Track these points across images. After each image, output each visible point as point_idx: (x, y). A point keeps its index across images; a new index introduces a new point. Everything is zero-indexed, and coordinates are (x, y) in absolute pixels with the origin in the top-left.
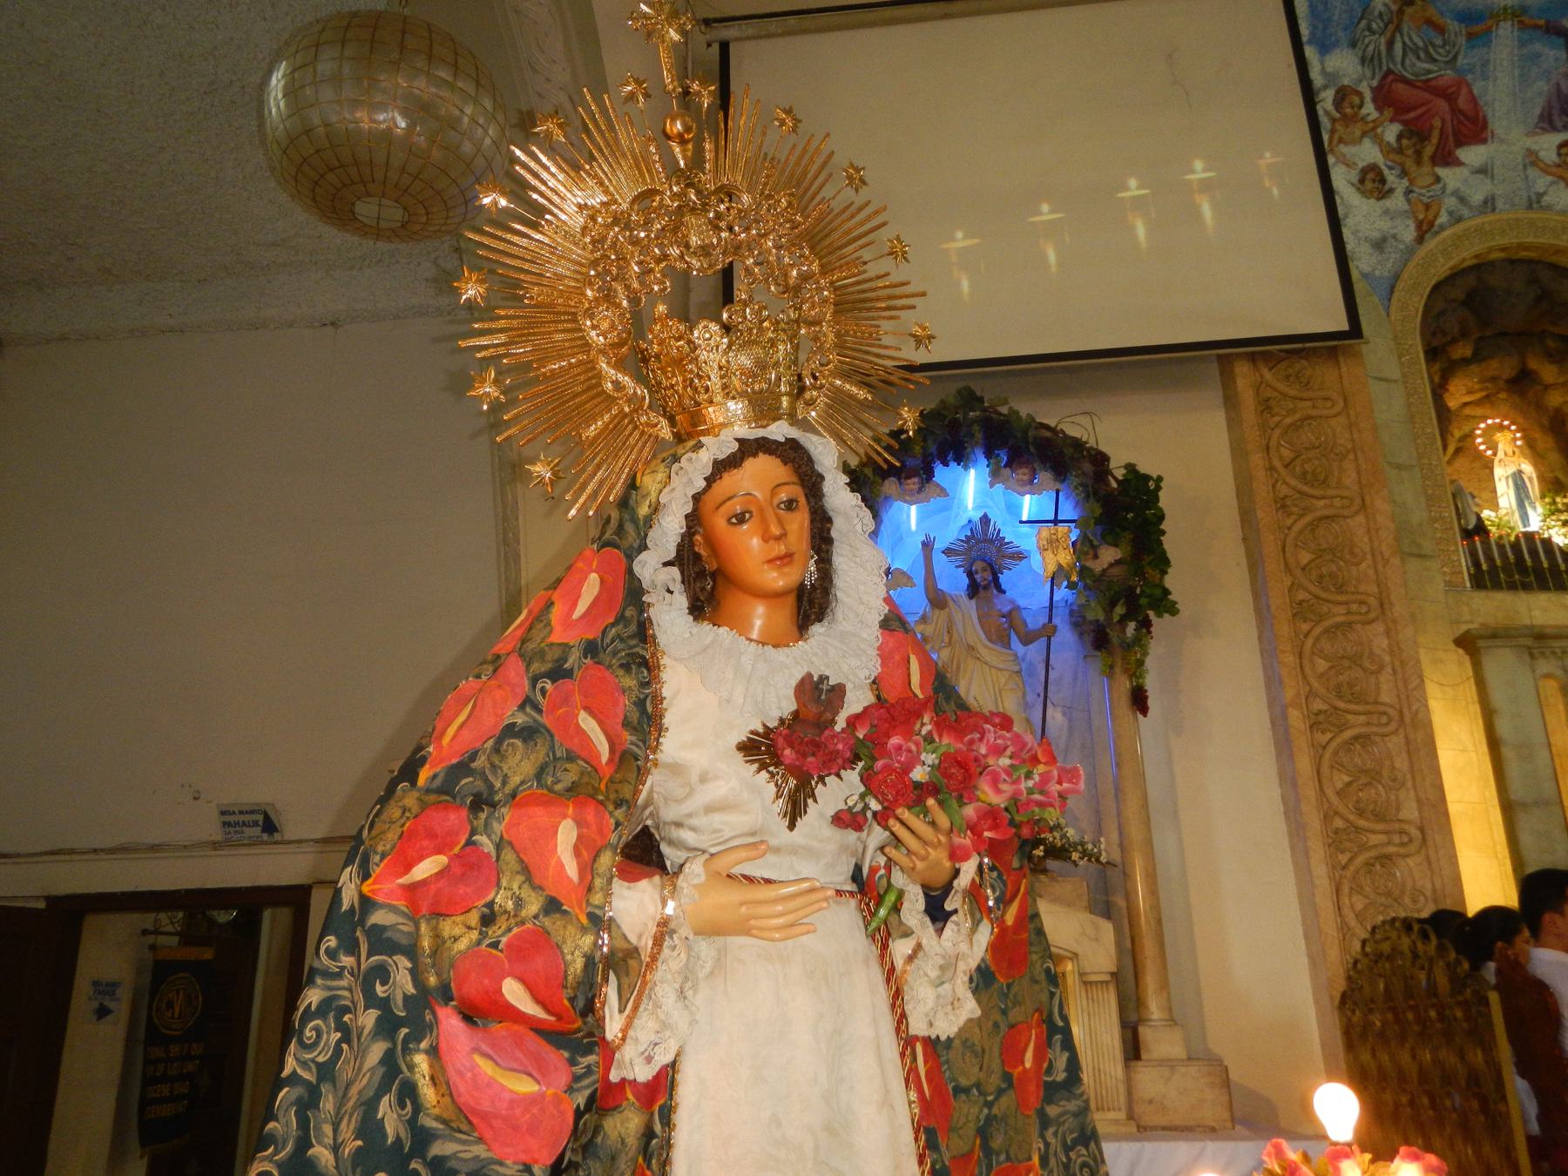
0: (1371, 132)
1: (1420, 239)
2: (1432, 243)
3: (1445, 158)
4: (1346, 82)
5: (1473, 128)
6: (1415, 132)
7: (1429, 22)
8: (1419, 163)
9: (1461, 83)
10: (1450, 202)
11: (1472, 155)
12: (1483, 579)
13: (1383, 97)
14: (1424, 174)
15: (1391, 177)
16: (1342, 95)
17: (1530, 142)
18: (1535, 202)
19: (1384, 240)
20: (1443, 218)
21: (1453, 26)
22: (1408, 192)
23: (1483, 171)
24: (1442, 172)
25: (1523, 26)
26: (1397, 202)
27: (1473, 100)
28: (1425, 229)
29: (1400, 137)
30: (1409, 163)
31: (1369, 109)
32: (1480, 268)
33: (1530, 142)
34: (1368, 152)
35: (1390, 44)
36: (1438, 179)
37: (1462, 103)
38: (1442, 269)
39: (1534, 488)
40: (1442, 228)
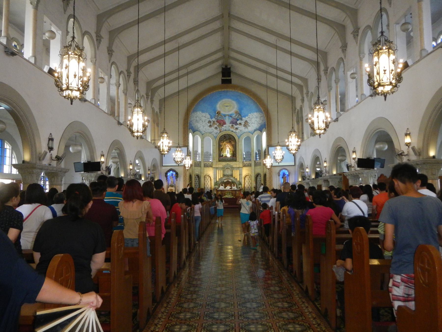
0: (216, 124)
1: (220, 133)
2: (220, 133)
3: (222, 126)
5: (225, 123)
6: (220, 124)
10: (223, 129)
11: (225, 126)
12: (219, 161)
13: (217, 121)
14: (220, 127)
15: (218, 128)
16: (213, 122)
17: (229, 125)
20: (222, 131)
21: (223, 116)
24: (222, 127)
26: (218, 129)
28: (220, 132)
31: (216, 122)
33: (229, 125)
34: (216, 126)
37: (224, 121)
39: (229, 152)
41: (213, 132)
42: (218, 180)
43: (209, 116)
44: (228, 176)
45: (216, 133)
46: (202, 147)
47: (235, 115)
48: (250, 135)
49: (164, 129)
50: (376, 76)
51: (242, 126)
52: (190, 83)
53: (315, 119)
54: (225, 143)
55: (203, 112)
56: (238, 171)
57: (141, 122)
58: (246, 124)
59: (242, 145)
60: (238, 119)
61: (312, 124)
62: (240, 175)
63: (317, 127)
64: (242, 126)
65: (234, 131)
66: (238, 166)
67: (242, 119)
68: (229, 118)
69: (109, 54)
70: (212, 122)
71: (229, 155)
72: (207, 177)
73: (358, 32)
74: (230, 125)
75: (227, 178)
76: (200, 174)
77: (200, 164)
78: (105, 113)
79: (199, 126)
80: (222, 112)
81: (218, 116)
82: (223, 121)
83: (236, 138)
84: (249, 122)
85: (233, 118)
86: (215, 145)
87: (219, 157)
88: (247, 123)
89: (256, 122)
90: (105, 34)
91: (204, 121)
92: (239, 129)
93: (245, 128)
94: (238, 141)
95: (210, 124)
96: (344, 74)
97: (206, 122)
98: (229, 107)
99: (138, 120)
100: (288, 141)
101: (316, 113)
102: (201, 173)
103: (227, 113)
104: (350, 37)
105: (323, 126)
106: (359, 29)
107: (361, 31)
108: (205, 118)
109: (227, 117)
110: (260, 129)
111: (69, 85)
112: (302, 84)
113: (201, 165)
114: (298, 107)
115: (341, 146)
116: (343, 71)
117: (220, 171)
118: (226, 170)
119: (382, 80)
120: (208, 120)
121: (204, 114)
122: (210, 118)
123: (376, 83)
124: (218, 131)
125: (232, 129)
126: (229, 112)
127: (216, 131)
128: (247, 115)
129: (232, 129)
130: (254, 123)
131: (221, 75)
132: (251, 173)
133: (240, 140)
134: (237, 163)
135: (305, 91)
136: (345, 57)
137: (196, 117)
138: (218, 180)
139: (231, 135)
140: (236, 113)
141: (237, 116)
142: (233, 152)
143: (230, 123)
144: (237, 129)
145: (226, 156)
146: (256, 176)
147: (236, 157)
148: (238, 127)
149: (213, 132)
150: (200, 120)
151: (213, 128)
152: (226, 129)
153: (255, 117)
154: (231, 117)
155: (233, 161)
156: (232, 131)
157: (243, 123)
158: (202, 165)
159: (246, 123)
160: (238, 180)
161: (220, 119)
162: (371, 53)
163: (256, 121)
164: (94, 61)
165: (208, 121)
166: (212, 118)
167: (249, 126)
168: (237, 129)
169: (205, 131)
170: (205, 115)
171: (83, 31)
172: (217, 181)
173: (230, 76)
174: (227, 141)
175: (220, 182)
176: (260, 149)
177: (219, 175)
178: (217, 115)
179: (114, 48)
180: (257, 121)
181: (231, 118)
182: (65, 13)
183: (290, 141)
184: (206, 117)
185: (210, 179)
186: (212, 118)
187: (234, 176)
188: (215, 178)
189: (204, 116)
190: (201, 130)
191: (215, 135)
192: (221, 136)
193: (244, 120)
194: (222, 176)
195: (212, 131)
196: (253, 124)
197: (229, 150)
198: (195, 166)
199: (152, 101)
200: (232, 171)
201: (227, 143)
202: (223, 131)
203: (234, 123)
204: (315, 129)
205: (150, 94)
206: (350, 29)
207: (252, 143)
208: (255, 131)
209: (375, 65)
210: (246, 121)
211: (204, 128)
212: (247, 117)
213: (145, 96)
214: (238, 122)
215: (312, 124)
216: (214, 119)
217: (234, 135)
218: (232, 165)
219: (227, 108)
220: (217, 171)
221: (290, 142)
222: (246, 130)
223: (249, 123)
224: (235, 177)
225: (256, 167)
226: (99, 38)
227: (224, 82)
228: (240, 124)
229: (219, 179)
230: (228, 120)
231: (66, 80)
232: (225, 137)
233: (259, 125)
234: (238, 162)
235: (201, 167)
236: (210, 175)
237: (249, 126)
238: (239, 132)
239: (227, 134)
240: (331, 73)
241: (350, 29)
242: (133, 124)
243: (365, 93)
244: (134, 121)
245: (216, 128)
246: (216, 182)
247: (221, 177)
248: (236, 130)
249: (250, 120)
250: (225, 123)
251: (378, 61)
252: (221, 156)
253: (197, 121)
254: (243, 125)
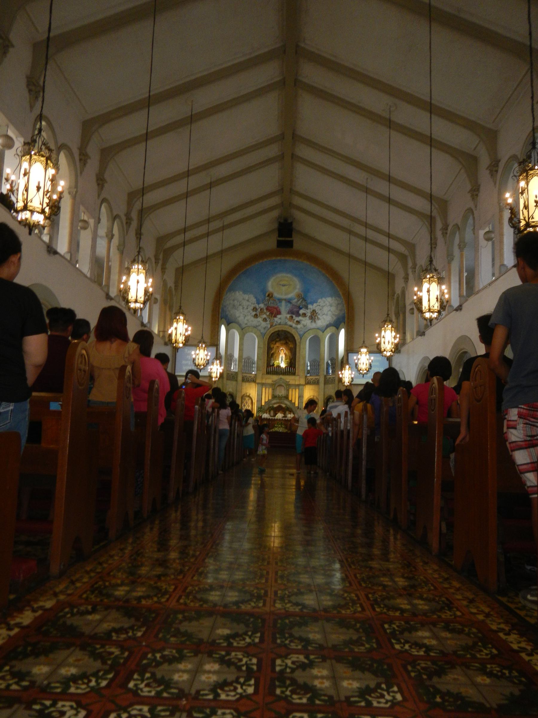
0: (265, 313)
1: (271, 327)
3: (275, 316)
4: (262, 307)
5: (279, 313)
6: (272, 313)
7: (274, 300)
8: (272, 317)
9: (278, 307)
10: (275, 323)
11: (279, 316)
12: (268, 373)
13: (267, 309)
14: (272, 318)
15: (268, 319)
17: (286, 315)
18: (286, 324)
19: (265, 328)
20: (274, 324)
21: (277, 300)
22: (270, 321)
23: (280, 318)
25: (286, 301)
26: (268, 322)
27: (279, 309)
28: (271, 326)
29: (269, 314)
30: (270, 317)
31: (265, 311)
32: (279, 331)
33: (286, 315)
34: (265, 316)
35: (268, 302)
36: (274, 319)
38: (273, 332)
39: (284, 359)
40: (274, 326)
41: (259, 325)
42: (263, 404)
43: (254, 300)
44: (280, 398)
45: (265, 328)
46: (241, 350)
47: (296, 300)
48: (320, 333)
49: (179, 308)
50: (522, 211)
51: (307, 318)
52: (226, 245)
53: (424, 294)
54: (278, 344)
55: (245, 292)
56: (297, 390)
57: (142, 286)
58: (314, 316)
59: (305, 348)
60: (301, 306)
61: (418, 303)
62: (301, 397)
63: (427, 308)
64: (307, 318)
65: (294, 325)
66: (297, 383)
67: (307, 308)
68: (286, 306)
69: (98, 184)
70: (259, 310)
71: (283, 365)
72: (247, 399)
73: (498, 166)
74: (288, 316)
75: (278, 401)
76: (235, 393)
77: (235, 377)
78: (86, 276)
79: (237, 315)
80: (276, 295)
81: (269, 300)
82: (276, 308)
83: (297, 337)
84: (319, 312)
85: (293, 305)
86: (262, 346)
87: (267, 367)
88: (315, 314)
89: (330, 312)
90: (93, 152)
91: (246, 307)
92: (303, 322)
93: (312, 322)
94: (300, 343)
95: (254, 313)
96: (474, 234)
97: (249, 309)
98: (287, 287)
99: (138, 282)
100: (380, 336)
101: (426, 286)
102: (236, 391)
103: (284, 297)
104: (484, 175)
105: (436, 306)
106: (500, 161)
107: (502, 165)
108: (248, 303)
109: (283, 303)
110: (337, 325)
111: (27, 203)
112: (406, 253)
113: (237, 378)
114: (398, 291)
115: (466, 351)
116: (472, 230)
117: (267, 389)
118: (278, 388)
119: (533, 218)
120: (253, 306)
121: (246, 297)
122: (256, 302)
123: (523, 223)
124: (267, 324)
125: (290, 323)
126: (286, 294)
127: (264, 324)
128: (315, 302)
129: (290, 323)
130: (327, 315)
131: (276, 234)
132: (319, 395)
133: (302, 341)
134: (297, 378)
135: (410, 264)
136: (476, 206)
137: (234, 300)
138: (263, 404)
139: (289, 333)
140: (299, 296)
141: (300, 302)
142: (291, 360)
143: (288, 313)
144: (298, 322)
145: (279, 366)
146: (326, 401)
147: (295, 367)
148: (301, 320)
149: (259, 325)
150: (240, 305)
151: (260, 319)
152: (280, 323)
153: (328, 304)
154: (291, 303)
155: (289, 375)
156: (291, 326)
157: (309, 314)
158: (240, 378)
159: (313, 314)
160: (297, 405)
161: (272, 305)
162: (515, 176)
163: (330, 310)
164: (74, 193)
165: (253, 308)
166: (258, 303)
167: (318, 319)
168: (298, 322)
169: (246, 324)
170: (248, 297)
171: (59, 145)
172: (261, 405)
173: (291, 236)
174: (282, 342)
175: (267, 407)
176: (335, 357)
177: (266, 396)
178: (267, 298)
179: (107, 176)
180: (331, 312)
181: (289, 305)
182: (31, 111)
183: (382, 336)
184: (249, 300)
185: (250, 401)
186: (258, 303)
187: (290, 399)
188: (259, 400)
189: (247, 299)
190: (241, 322)
191: (262, 331)
192: (272, 334)
193: (311, 309)
194: (270, 398)
195: (258, 325)
196: (324, 316)
197: (284, 356)
198: (227, 379)
199: (163, 269)
200: (288, 391)
201: (282, 344)
202: (276, 325)
203: (295, 312)
204: (424, 311)
205: (161, 256)
206: (485, 161)
207: (322, 346)
208: (328, 326)
209: (522, 193)
210: (314, 311)
211: (246, 318)
212: (315, 305)
213: (153, 260)
214: (301, 312)
215: (418, 303)
216: (262, 305)
217: (293, 332)
218: (288, 380)
219: (284, 288)
220: (264, 389)
221: (383, 337)
222: (313, 325)
223: (319, 314)
224: (291, 401)
225: (326, 386)
226: (84, 158)
227: (280, 244)
228: (304, 315)
229: (265, 402)
230: (284, 308)
231: (23, 194)
232: (278, 334)
233: (335, 318)
234: (299, 377)
235: (236, 381)
236: (251, 396)
237: (318, 319)
238: (301, 328)
239: (282, 331)
240: (453, 234)
241: (485, 161)
242: (129, 289)
243: (505, 263)
244: (132, 283)
245: (265, 320)
246: (260, 406)
248: (297, 324)
249: (320, 310)
250: (279, 313)
251: (526, 186)
252: (271, 366)
253: (234, 306)
254: (308, 316)
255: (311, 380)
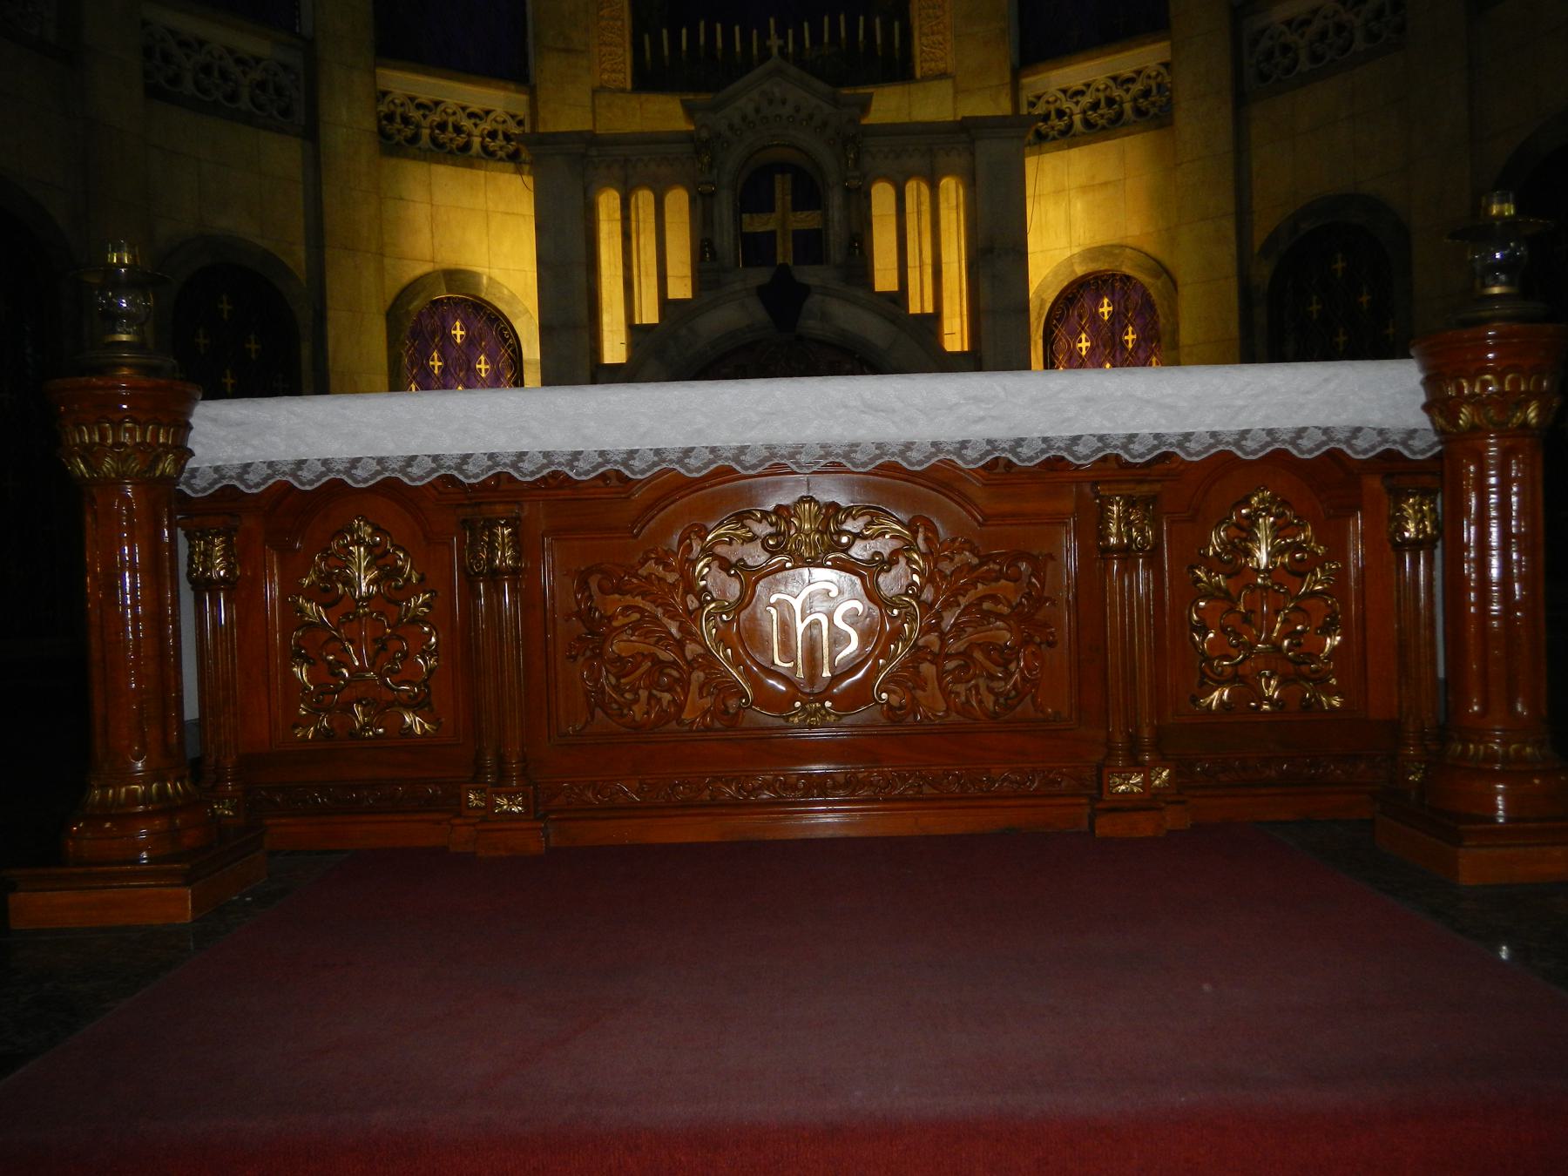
56: (951, 190)
76: (297, 257)
117: (644, 200)
146: (1263, 273)
187: (885, 281)
194: (680, 289)
220: (608, 204)
224: (899, 297)
229: (636, 332)
234: (946, 85)
235: (311, 133)
247: (665, 303)
255: (1066, 105)
